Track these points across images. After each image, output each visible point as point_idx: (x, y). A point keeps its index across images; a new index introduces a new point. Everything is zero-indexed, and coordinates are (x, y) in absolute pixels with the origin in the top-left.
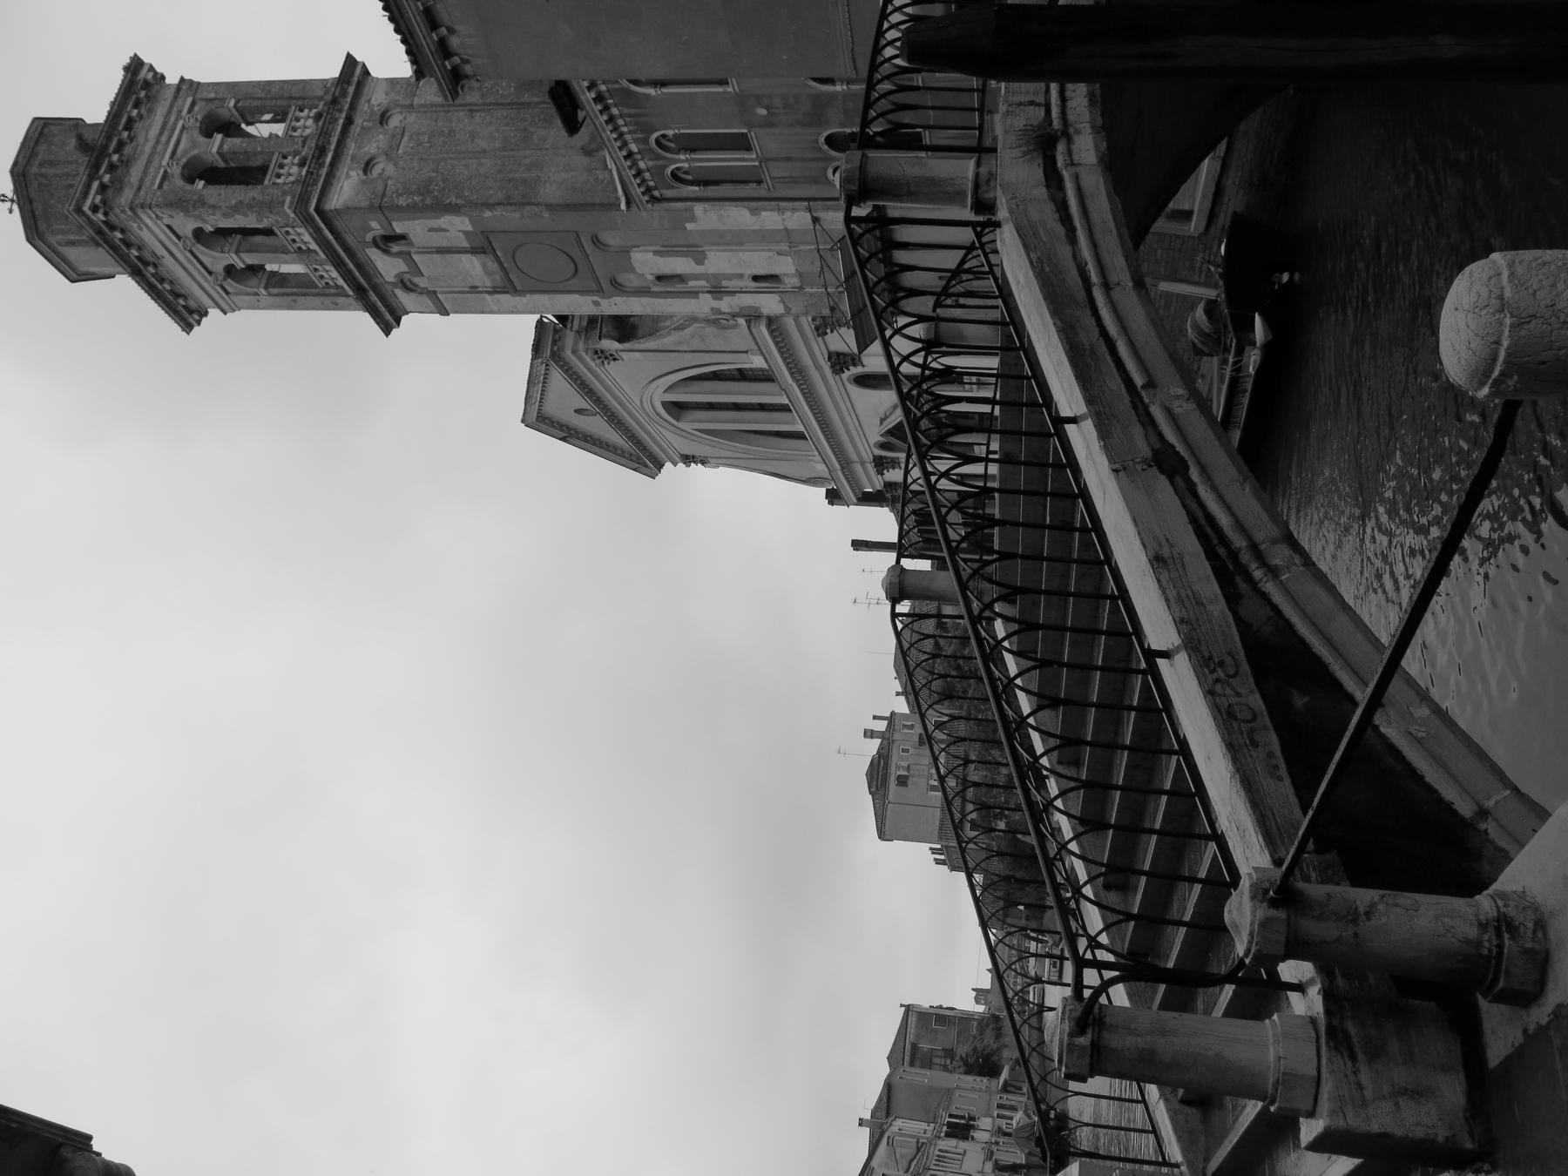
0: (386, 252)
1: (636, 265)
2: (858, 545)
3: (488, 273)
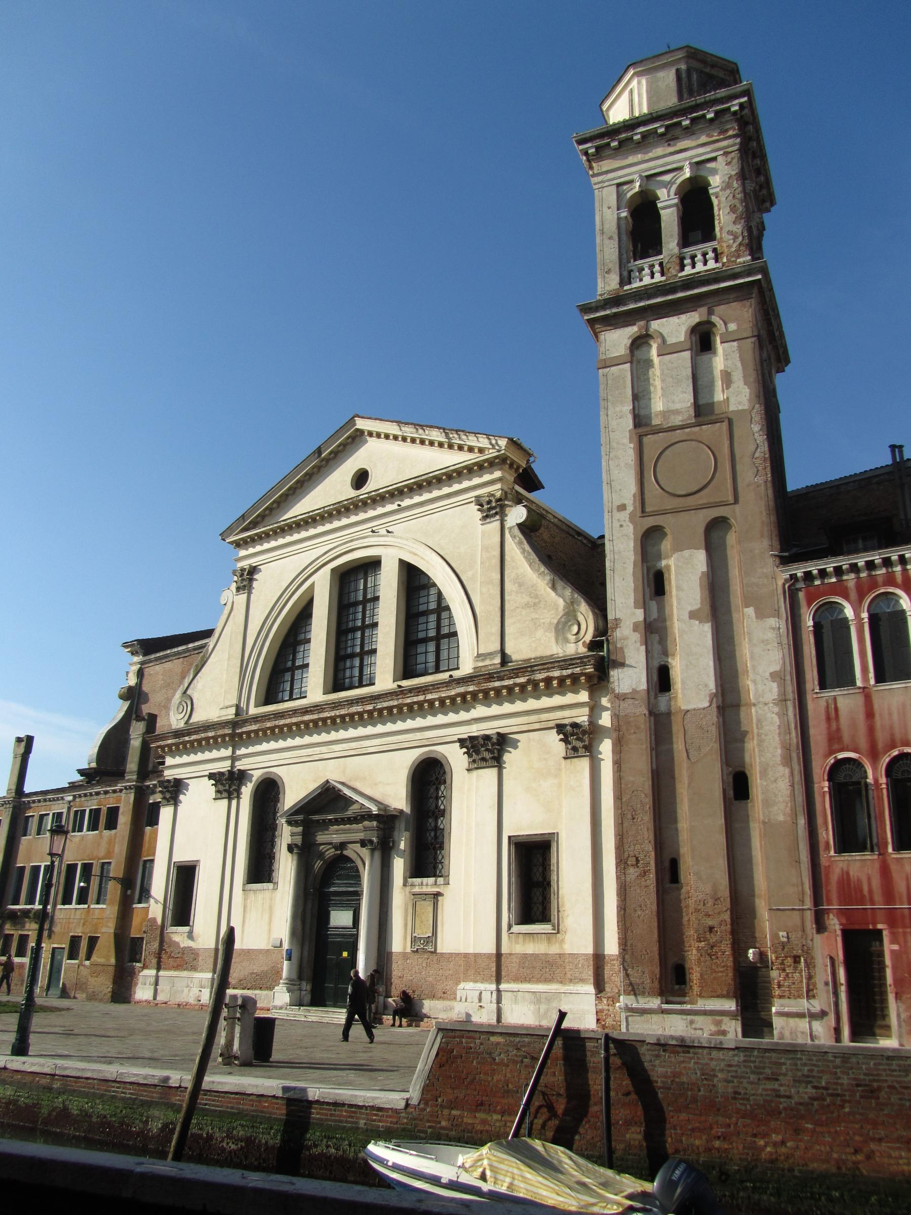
0: (694, 330)
1: (686, 553)
2: (28, 743)
3: (665, 414)
